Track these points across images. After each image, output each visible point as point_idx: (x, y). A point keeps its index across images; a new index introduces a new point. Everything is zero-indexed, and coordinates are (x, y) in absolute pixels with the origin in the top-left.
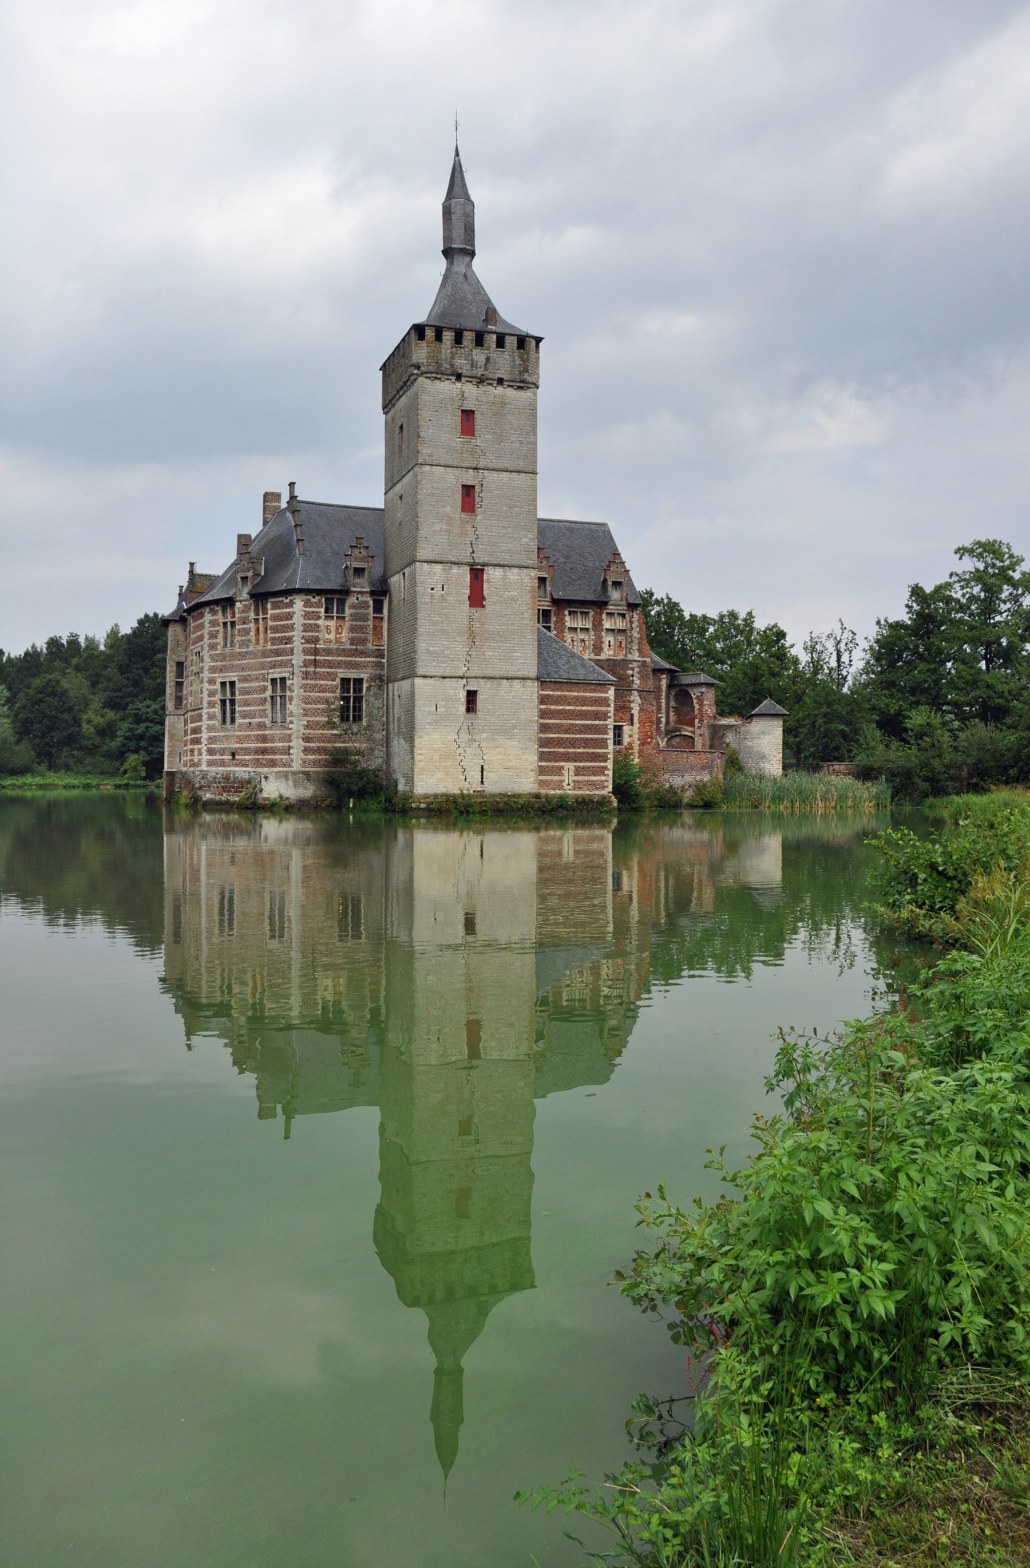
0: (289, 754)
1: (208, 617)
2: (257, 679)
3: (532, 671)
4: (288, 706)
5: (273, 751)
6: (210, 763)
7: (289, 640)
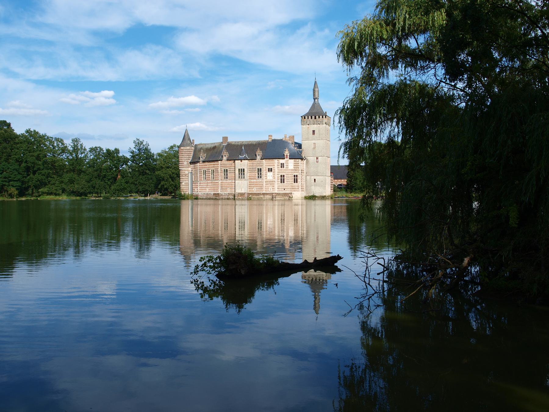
2: (291, 175)
3: (330, 175)
5: (295, 188)
6: (278, 191)
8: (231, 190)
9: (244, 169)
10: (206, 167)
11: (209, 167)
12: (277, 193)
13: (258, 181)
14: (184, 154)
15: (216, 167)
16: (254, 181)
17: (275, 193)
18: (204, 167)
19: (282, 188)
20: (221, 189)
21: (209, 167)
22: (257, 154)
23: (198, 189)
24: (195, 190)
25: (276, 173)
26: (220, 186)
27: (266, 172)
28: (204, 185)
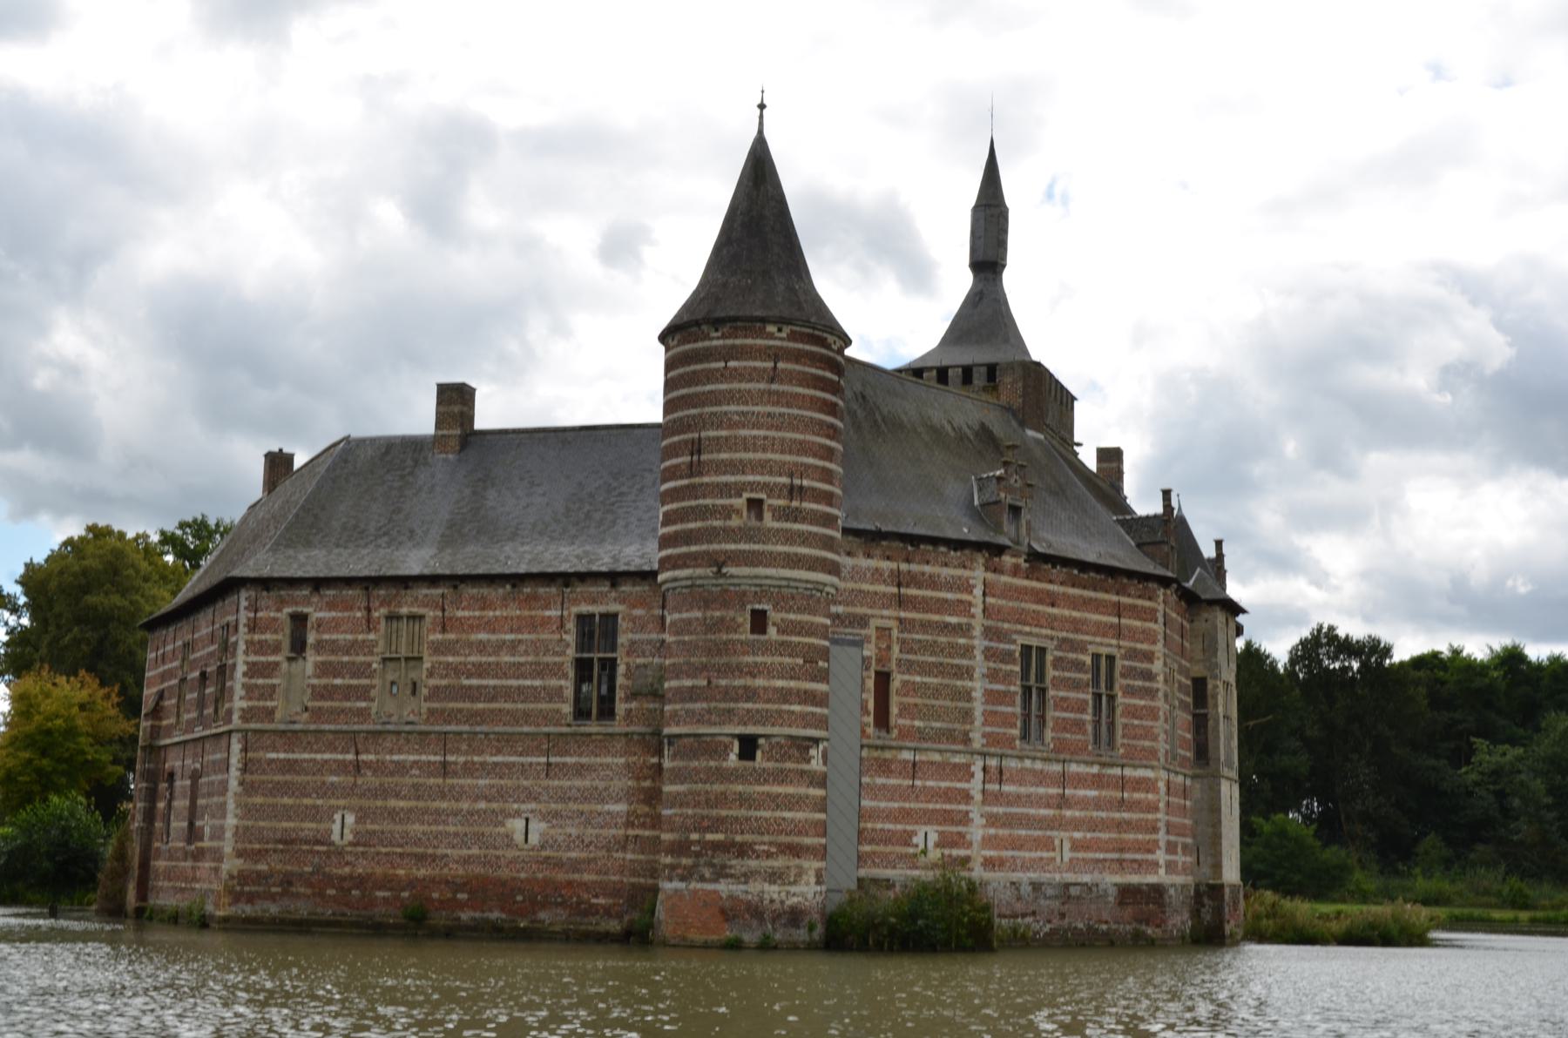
10: (1052, 622)
11: (1077, 626)
15: (1133, 634)
18: (1037, 619)
21: (1074, 621)
23: (976, 832)
24: (906, 837)
28: (1029, 800)
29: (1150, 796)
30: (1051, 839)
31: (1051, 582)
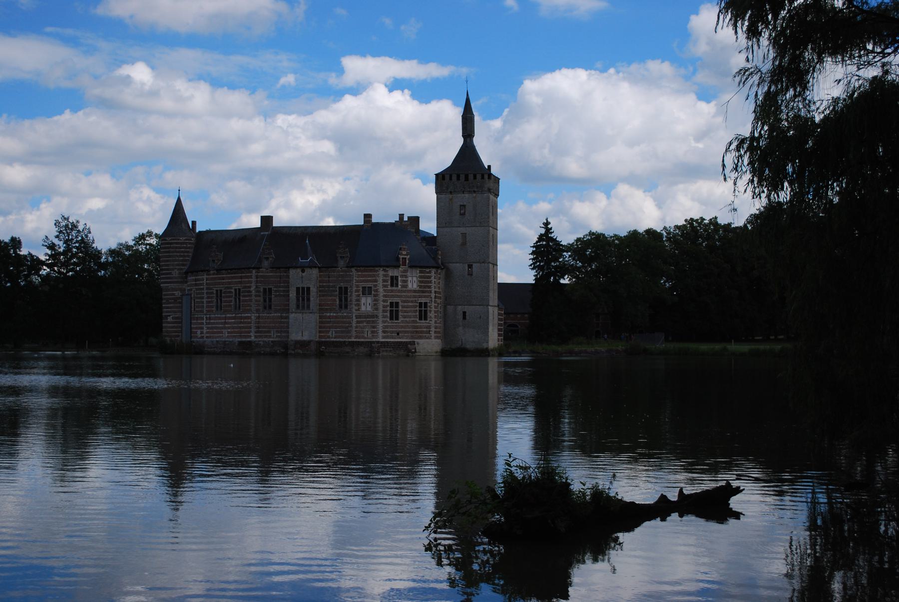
0: (430, 334)
1: (381, 273)
2: (412, 302)
4: (429, 314)
5: (422, 332)
6: (384, 337)
7: (430, 287)
8: (279, 334)
9: (308, 289)
10: (223, 284)
11: (230, 283)
12: (382, 342)
13: (341, 314)
14: (173, 252)
16: (332, 314)
17: (378, 342)
19: (393, 332)
20: (256, 332)
21: (228, 282)
22: (338, 255)
23: (205, 331)
24: (196, 333)
25: (382, 298)
26: (253, 325)
27: (358, 296)
28: (217, 323)
29: (249, 320)
30: (222, 332)
31: (223, 275)
